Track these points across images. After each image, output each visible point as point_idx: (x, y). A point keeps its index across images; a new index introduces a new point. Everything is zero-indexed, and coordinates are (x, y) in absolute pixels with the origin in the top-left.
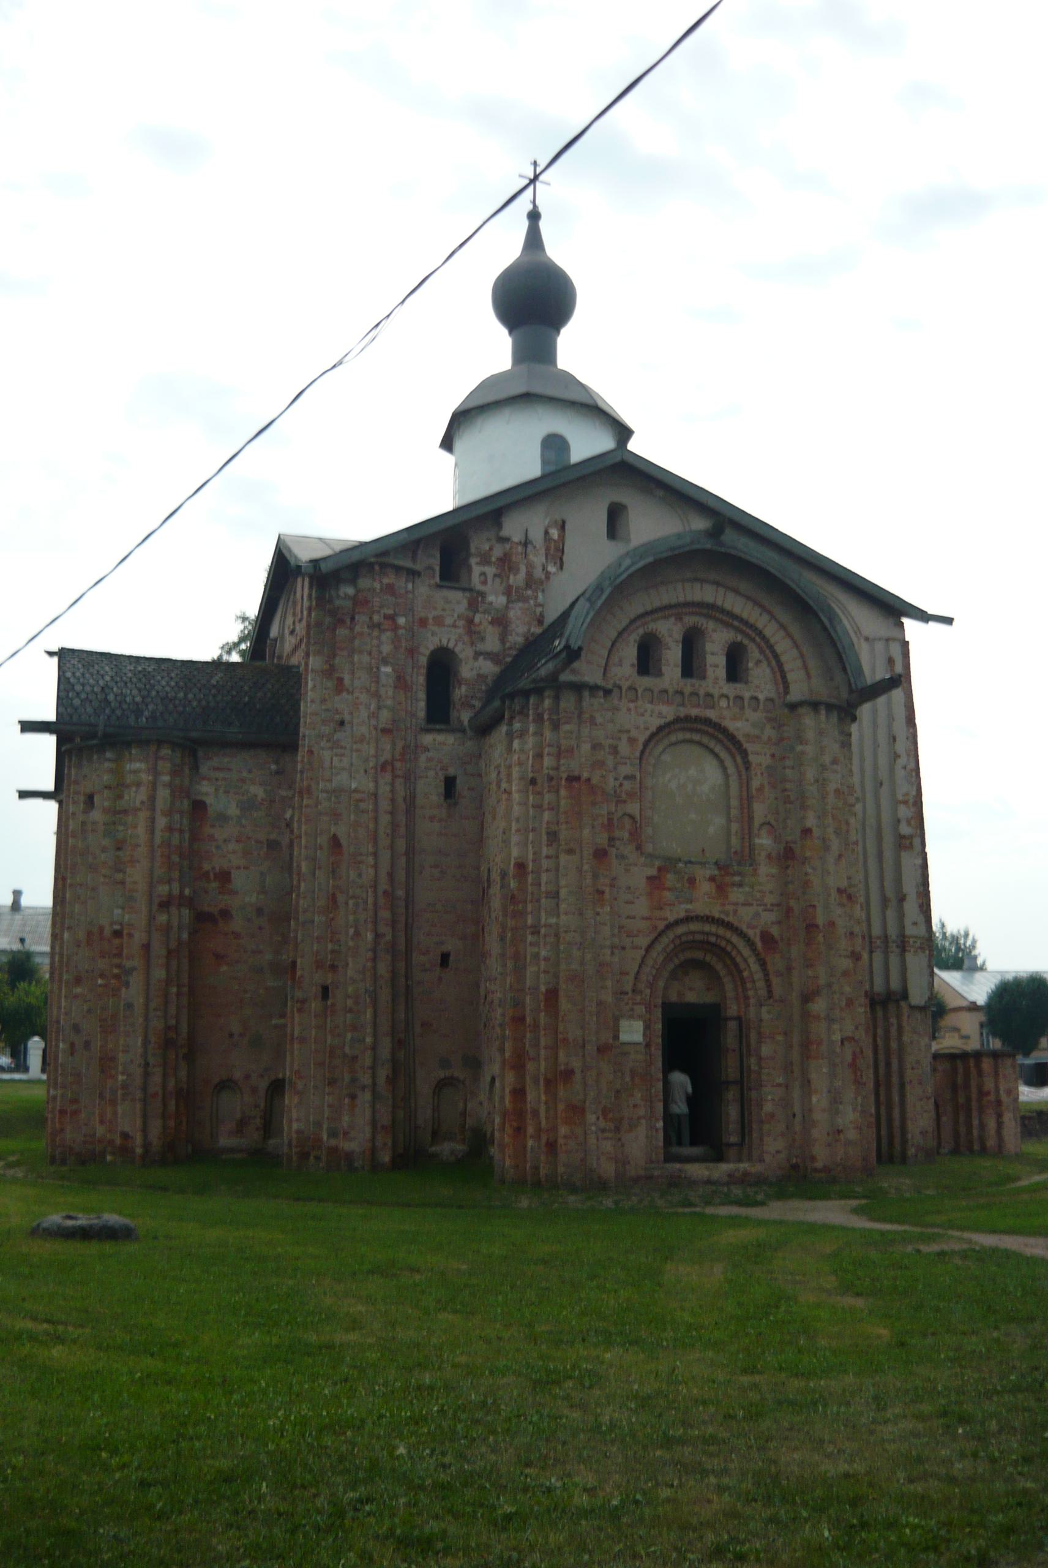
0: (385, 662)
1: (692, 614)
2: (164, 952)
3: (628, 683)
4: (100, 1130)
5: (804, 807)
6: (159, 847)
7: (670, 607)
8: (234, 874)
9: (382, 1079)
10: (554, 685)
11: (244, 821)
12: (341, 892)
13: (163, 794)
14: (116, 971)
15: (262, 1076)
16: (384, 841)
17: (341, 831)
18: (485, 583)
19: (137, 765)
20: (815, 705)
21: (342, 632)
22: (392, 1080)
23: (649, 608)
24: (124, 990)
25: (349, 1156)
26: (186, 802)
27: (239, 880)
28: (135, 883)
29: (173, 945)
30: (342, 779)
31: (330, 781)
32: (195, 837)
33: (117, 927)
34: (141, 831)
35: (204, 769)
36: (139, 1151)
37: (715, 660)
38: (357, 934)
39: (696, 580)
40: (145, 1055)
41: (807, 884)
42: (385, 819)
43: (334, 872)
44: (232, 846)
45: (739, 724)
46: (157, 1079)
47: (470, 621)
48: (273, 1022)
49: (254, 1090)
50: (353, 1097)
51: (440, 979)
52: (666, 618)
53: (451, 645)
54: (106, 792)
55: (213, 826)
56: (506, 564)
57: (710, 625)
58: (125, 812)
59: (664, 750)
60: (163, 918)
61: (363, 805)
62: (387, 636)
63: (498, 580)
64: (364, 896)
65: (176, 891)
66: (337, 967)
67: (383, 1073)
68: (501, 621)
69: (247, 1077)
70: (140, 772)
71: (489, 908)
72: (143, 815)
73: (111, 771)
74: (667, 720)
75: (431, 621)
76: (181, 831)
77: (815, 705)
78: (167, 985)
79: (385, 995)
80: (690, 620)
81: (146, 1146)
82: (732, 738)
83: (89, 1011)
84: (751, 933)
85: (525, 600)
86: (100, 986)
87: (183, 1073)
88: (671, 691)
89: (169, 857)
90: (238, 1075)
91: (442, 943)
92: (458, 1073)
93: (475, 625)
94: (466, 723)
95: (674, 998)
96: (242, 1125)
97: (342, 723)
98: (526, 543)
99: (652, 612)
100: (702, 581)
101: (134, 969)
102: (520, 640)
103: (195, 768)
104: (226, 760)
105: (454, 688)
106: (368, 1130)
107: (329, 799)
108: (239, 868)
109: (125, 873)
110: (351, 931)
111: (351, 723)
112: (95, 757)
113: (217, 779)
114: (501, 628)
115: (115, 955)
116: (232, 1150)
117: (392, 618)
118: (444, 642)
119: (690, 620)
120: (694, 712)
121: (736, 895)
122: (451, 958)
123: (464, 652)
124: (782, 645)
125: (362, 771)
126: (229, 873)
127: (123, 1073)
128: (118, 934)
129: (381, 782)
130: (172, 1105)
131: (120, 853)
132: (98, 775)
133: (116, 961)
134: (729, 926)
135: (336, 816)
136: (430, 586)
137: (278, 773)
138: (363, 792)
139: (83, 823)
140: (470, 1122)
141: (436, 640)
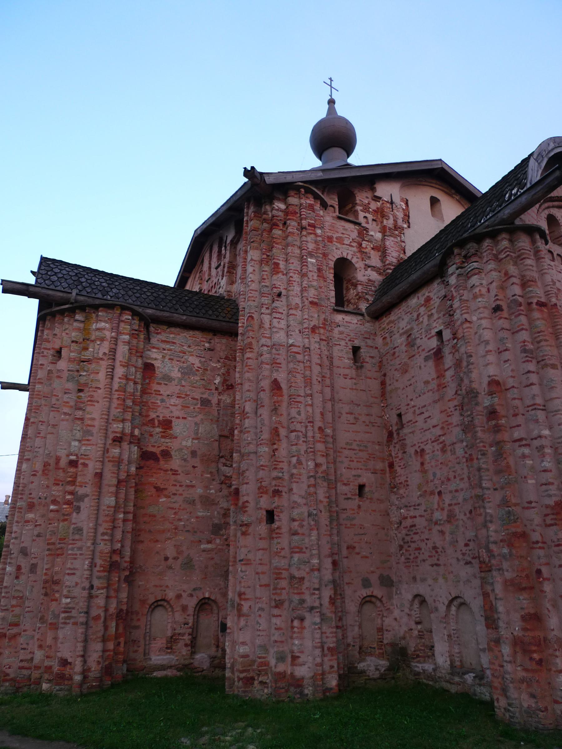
0: (311, 255)
2: (115, 482)
4: (39, 655)
6: (116, 391)
8: (175, 422)
9: (326, 601)
11: (183, 382)
12: (283, 427)
13: (122, 350)
14: (69, 497)
15: (191, 595)
16: (317, 387)
17: (281, 376)
18: (367, 223)
19: (102, 325)
21: (277, 232)
22: (332, 601)
24: (75, 514)
25: (298, 683)
26: (140, 361)
27: (178, 428)
28: (93, 419)
29: (123, 476)
30: (280, 337)
31: (270, 338)
32: (144, 392)
33: (73, 458)
34: (102, 376)
35: (154, 340)
36: (78, 678)
38: (299, 462)
40: (90, 578)
42: (316, 369)
43: (275, 410)
44: (173, 401)
46: (101, 601)
47: (360, 245)
48: (203, 546)
49: (184, 608)
50: (302, 619)
51: (359, 507)
53: (349, 257)
54: (74, 346)
55: (159, 384)
56: (380, 214)
58: (88, 361)
60: (116, 451)
61: (300, 357)
62: (311, 238)
63: (374, 223)
64: (303, 430)
65: (128, 431)
66: (281, 492)
67: (327, 593)
68: (382, 250)
69: (179, 597)
70: (104, 329)
71: (404, 446)
72: (104, 364)
73: (79, 329)
75: (335, 240)
76: (135, 383)
78: (115, 511)
79: (324, 519)
81: (85, 672)
83: (38, 536)
85: (395, 236)
86: (52, 511)
87: (124, 595)
89: (124, 400)
90: (171, 595)
91: (359, 476)
92: (378, 592)
93: (363, 248)
94: (364, 310)
96: (172, 641)
97: (279, 295)
98: (392, 203)
101: (87, 496)
102: (395, 261)
103: (148, 339)
104: (172, 336)
105: (348, 289)
106: (318, 652)
107: (270, 353)
108: (178, 418)
109: (84, 410)
110: (294, 460)
111: (287, 297)
112: (66, 320)
113: (164, 349)
114: (380, 253)
115: (69, 483)
116: (163, 668)
117: (313, 226)
118: (345, 255)
122: (367, 489)
123: (358, 263)
125: (298, 332)
126: (171, 422)
127: (67, 597)
128: (74, 464)
129: (312, 340)
130: (113, 625)
131: (81, 394)
132: (67, 334)
133: (70, 488)
135: (275, 364)
136: (333, 217)
137: (210, 349)
138: (299, 347)
139: (50, 372)
140: (388, 638)
141: (339, 252)
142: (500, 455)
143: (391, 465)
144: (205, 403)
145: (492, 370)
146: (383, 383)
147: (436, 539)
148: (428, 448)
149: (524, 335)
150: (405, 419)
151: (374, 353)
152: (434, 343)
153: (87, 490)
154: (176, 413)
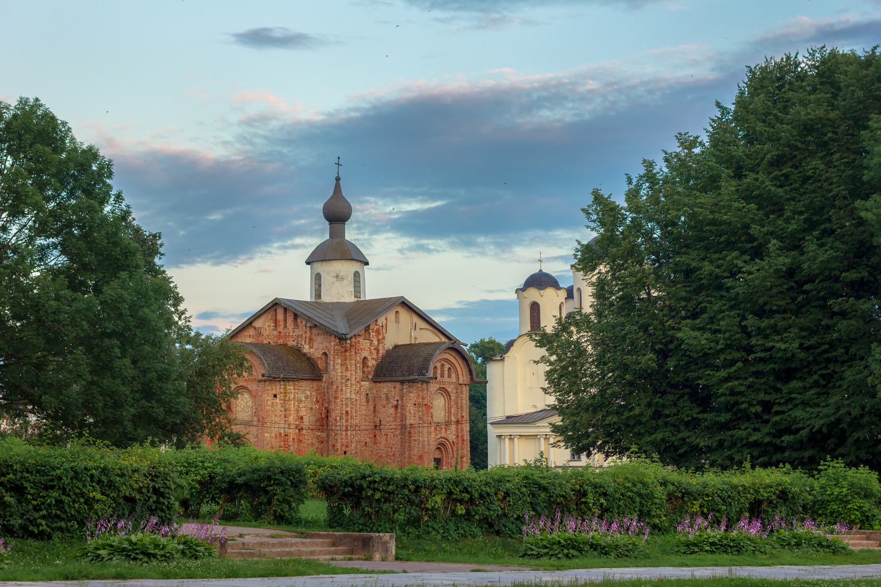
5: (462, 410)
10: (423, 382)
17: (349, 409)
20: (465, 385)
21: (348, 353)
27: (306, 419)
30: (348, 395)
37: (446, 372)
41: (462, 430)
43: (347, 421)
56: (378, 332)
57: (445, 363)
68: (377, 350)
77: (465, 385)
82: (448, 392)
121: (448, 432)
123: (369, 358)
124: (459, 369)
128: (286, 435)
134: (447, 439)
135: (347, 405)
142: (410, 443)
143: (375, 436)
144: (311, 409)
145: (411, 421)
146: (375, 407)
147: (388, 460)
148: (389, 434)
149: (420, 413)
150: (382, 423)
151: (372, 395)
152: (395, 403)
153: (291, 443)
154: (305, 414)
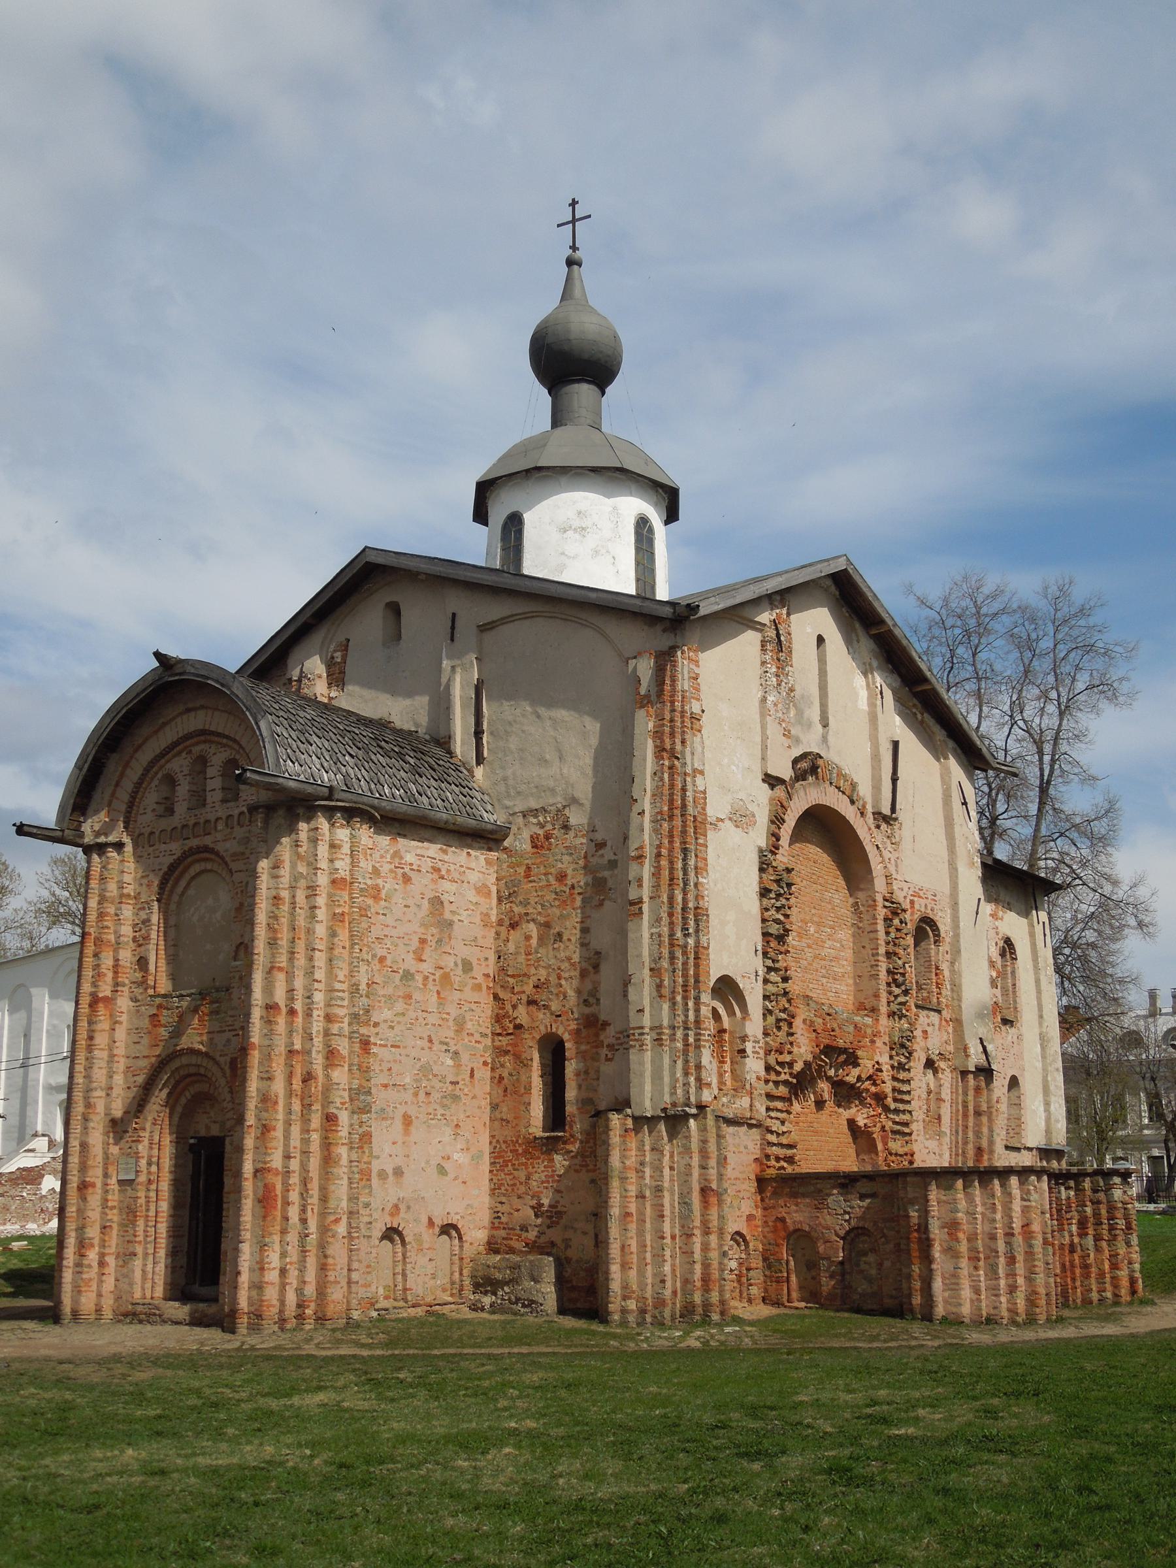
1: (197, 743)
3: (149, 830)
7: (175, 744)
23: (158, 751)
39: (188, 710)
45: (228, 845)
52: (179, 753)
59: (188, 884)
74: (175, 857)
80: (196, 750)
84: (222, 1060)
88: (179, 826)
95: (203, 1133)
99: (163, 754)
100: (195, 709)
119: (196, 750)
120: (195, 842)
